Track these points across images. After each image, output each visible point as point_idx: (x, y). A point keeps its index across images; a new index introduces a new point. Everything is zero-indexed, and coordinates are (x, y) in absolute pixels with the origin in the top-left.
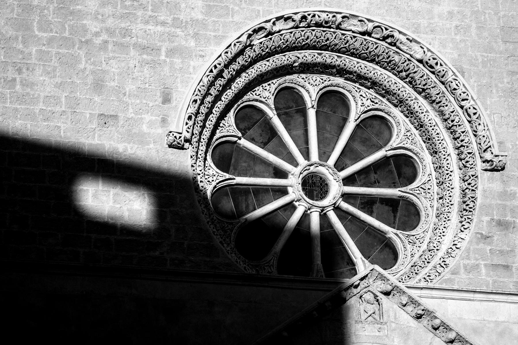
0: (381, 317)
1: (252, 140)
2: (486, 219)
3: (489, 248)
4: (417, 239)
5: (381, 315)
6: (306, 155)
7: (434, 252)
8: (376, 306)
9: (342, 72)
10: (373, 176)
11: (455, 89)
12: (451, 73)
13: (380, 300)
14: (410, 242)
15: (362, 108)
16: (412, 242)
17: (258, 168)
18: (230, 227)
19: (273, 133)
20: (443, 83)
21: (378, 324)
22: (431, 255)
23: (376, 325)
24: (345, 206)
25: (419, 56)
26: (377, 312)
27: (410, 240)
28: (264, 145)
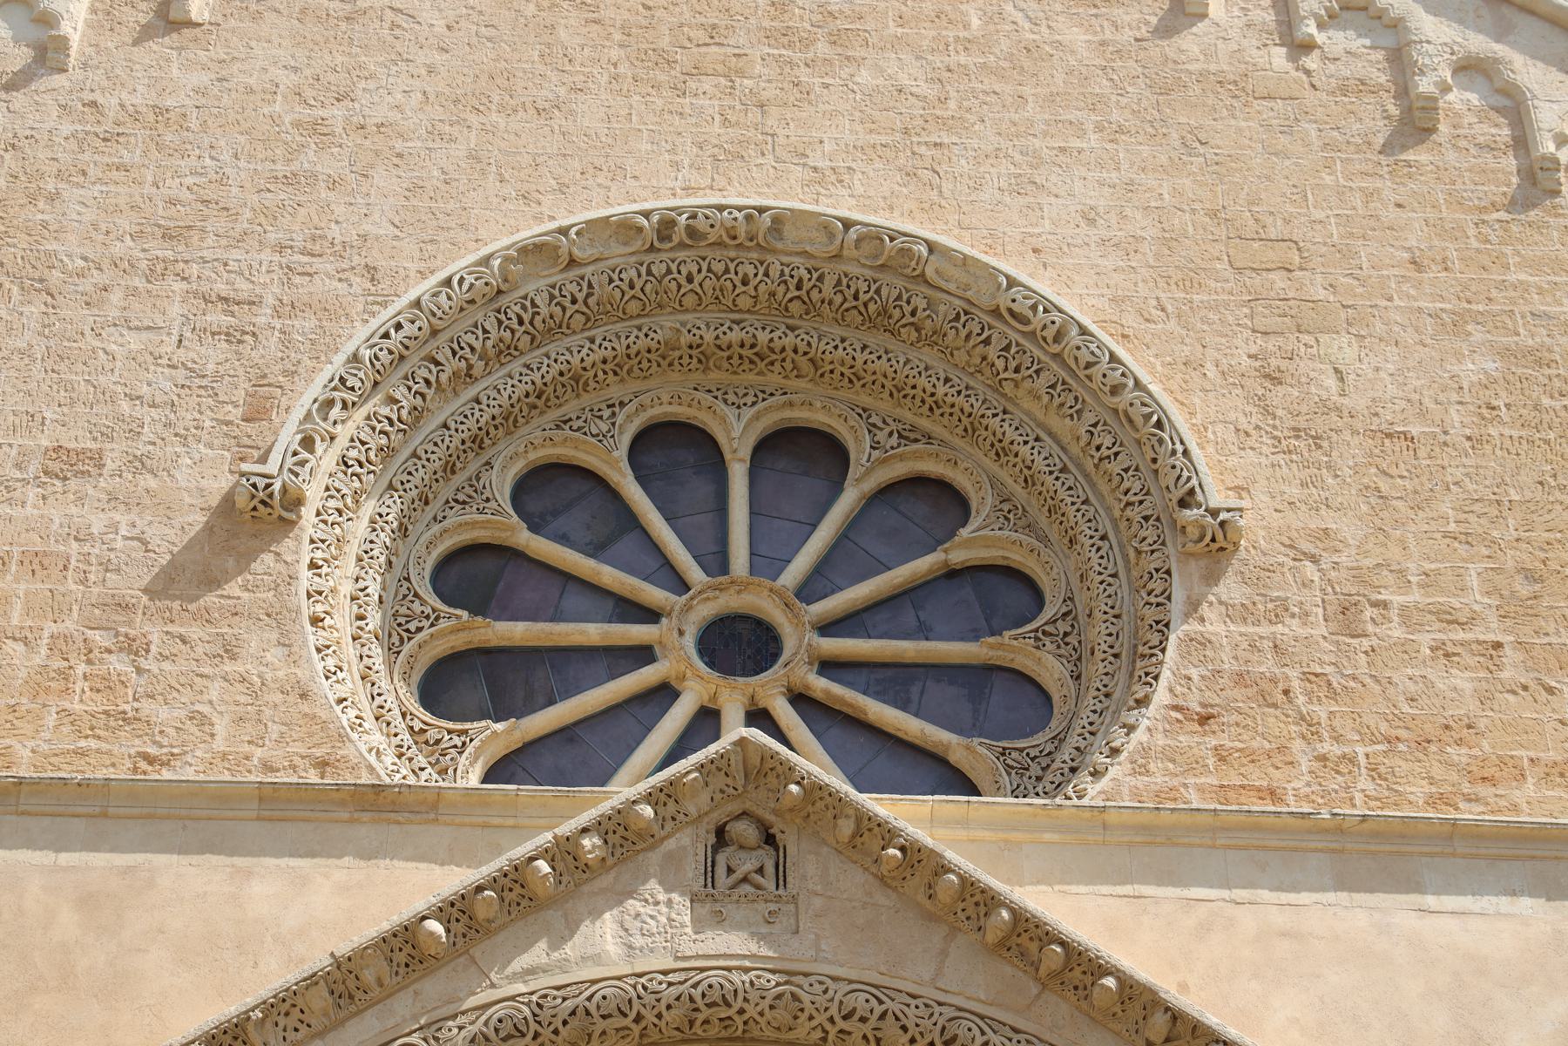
0: (781, 882)
1: (563, 539)
4: (1033, 759)
5: (781, 878)
6: (717, 562)
7: (1062, 774)
8: (766, 857)
10: (909, 618)
11: (1089, 365)
13: (779, 836)
14: (1012, 768)
15: (876, 454)
16: (1015, 765)
17: (573, 600)
18: (457, 741)
19: (629, 521)
20: (1057, 356)
21: (766, 901)
22: (1052, 783)
24: (820, 685)
27: (1009, 762)
28: (595, 550)
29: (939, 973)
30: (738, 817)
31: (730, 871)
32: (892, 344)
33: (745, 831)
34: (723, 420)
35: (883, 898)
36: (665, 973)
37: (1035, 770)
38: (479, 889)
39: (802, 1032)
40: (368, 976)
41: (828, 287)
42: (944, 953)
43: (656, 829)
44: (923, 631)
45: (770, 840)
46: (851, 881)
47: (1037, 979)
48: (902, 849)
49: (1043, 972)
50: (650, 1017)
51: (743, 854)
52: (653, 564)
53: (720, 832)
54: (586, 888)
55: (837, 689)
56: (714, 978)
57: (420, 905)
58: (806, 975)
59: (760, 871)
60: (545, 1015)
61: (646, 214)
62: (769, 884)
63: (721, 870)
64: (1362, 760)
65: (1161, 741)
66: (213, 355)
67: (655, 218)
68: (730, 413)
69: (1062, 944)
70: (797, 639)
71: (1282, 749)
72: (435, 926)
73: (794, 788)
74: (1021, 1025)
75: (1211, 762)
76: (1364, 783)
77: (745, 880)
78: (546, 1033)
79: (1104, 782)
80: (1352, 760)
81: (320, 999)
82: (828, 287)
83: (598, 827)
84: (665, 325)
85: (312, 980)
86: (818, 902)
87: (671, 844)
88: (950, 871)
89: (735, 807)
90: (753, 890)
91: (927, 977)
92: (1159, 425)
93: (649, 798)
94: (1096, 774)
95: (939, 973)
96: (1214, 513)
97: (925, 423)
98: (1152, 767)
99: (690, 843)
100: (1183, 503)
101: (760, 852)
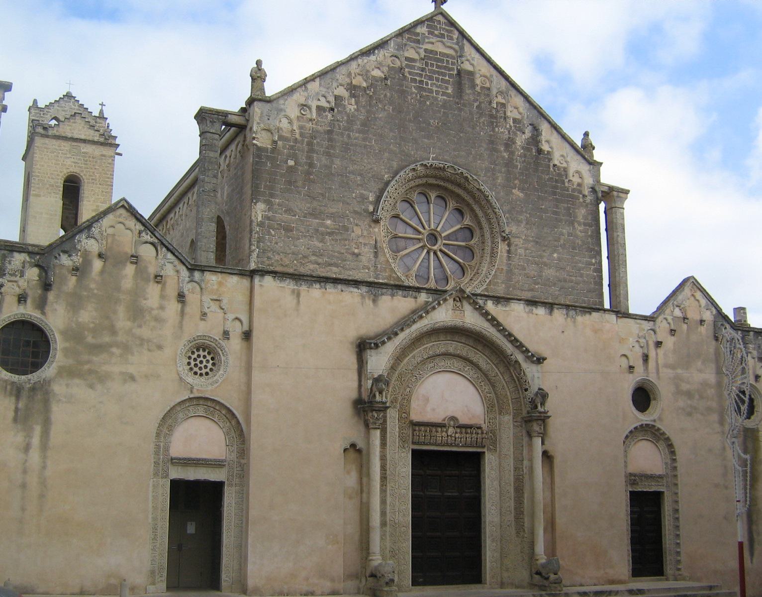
12: (490, 196)
34: (430, 196)
92: (500, 217)
100: (503, 232)
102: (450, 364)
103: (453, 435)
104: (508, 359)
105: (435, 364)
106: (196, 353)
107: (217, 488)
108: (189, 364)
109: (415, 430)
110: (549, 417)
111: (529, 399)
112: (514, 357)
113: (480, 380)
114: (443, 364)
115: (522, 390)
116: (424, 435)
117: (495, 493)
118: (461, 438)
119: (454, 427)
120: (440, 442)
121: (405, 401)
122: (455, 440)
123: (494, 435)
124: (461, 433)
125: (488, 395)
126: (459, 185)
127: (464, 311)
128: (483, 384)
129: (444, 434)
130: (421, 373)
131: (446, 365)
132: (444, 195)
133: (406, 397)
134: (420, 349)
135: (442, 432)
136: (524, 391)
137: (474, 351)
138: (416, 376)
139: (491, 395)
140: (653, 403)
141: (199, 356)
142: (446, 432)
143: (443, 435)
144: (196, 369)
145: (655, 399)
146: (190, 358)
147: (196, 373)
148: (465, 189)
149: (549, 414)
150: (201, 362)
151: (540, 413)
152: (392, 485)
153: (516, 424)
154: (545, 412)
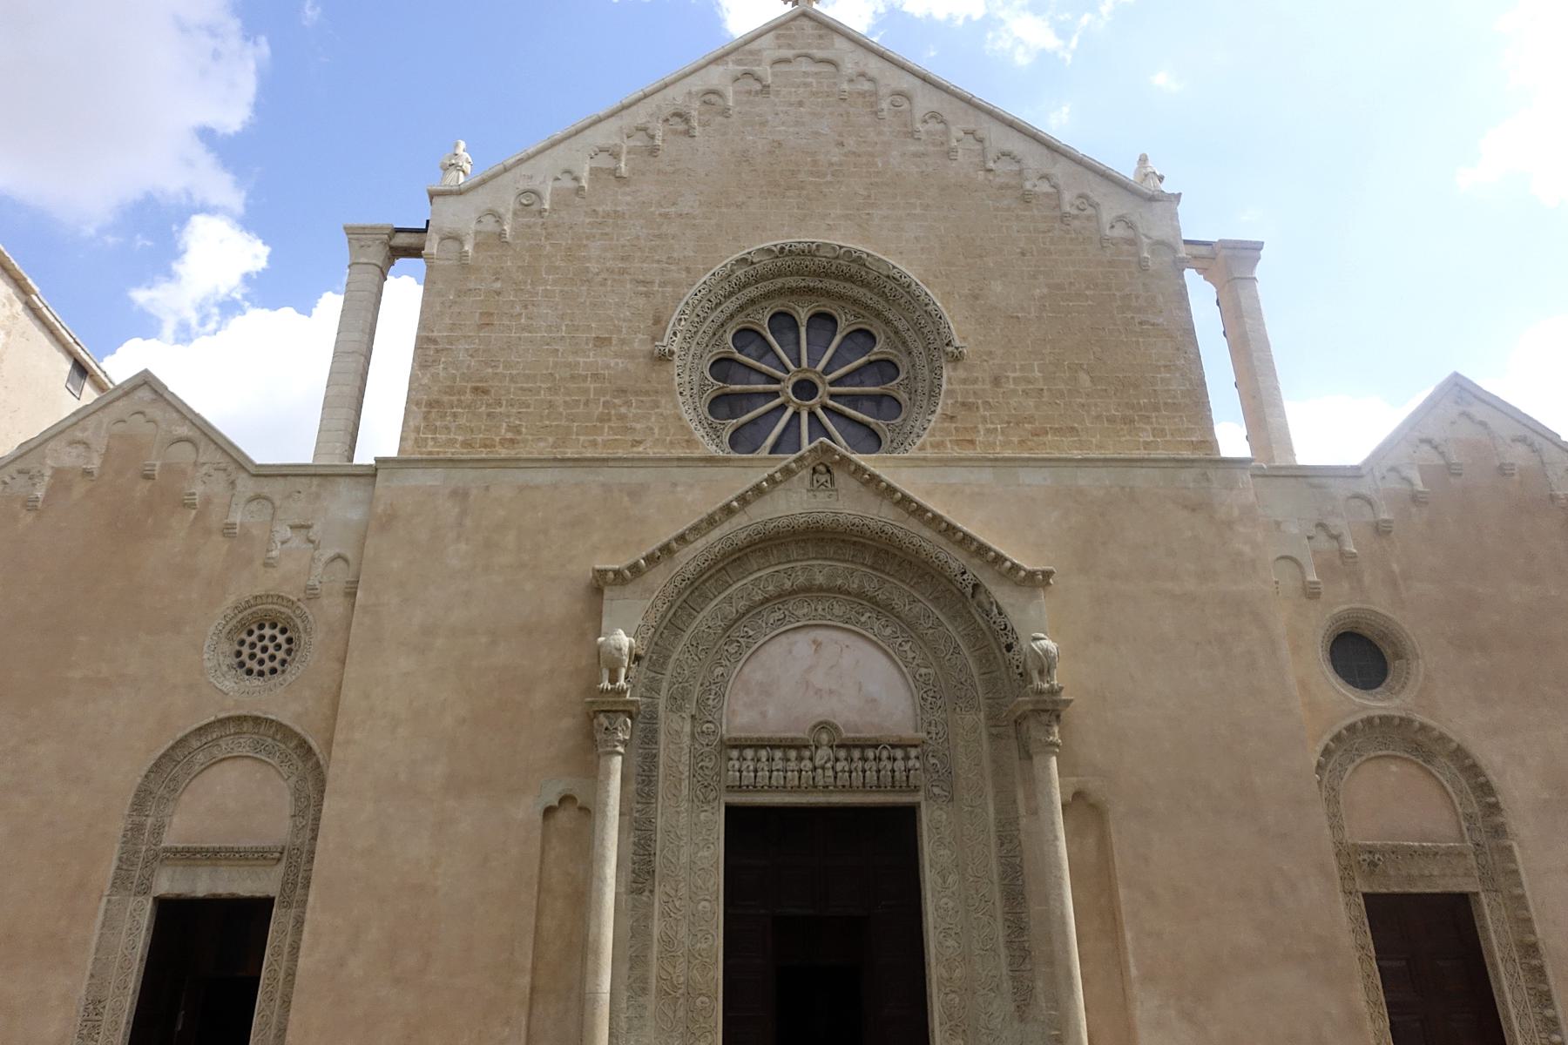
1: (748, 355)
2: (950, 402)
3: (954, 425)
5: (832, 483)
6: (798, 363)
8: (827, 477)
9: (828, 294)
10: (857, 380)
11: (918, 296)
12: (914, 285)
15: (847, 323)
17: (754, 377)
18: (722, 427)
19: (770, 348)
20: (908, 292)
23: (827, 493)
24: (831, 403)
25: (885, 273)
26: (829, 481)
28: (759, 359)
29: (879, 511)
30: (818, 465)
31: (818, 481)
32: (853, 286)
33: (822, 468)
34: (798, 312)
35: (863, 489)
36: (800, 514)
37: (897, 430)
38: (747, 492)
39: (840, 529)
40: (717, 518)
41: (833, 268)
42: (881, 505)
43: (796, 470)
44: (862, 384)
45: (828, 471)
46: (854, 484)
47: (908, 513)
48: (869, 475)
49: (910, 510)
50: (796, 527)
51: (821, 476)
52: (784, 369)
53: (814, 469)
54: (777, 489)
55: (836, 405)
56: (814, 515)
57: (731, 498)
58: (841, 513)
59: (827, 482)
60: (766, 528)
61: (775, 246)
62: (829, 485)
63: (815, 482)
64: (999, 430)
65: (939, 425)
66: (642, 301)
67: (778, 247)
68: (800, 310)
69: (916, 503)
70: (824, 390)
71: (976, 427)
72: (735, 504)
73: (837, 457)
74: (902, 525)
75: (954, 432)
76: (1000, 438)
77: (822, 484)
78: (767, 532)
79: (921, 440)
80: (996, 429)
81: (704, 525)
82: (833, 268)
83: (781, 470)
84: (779, 282)
85: (702, 521)
86: (844, 491)
87: (800, 474)
88: (882, 481)
89: (818, 462)
90: (824, 487)
91: (875, 512)
92: (940, 318)
93: (795, 461)
94: (919, 436)
95: (879, 511)
96: (957, 348)
97: (862, 312)
98: (936, 434)
99: (806, 473)
100: (947, 345)
101: (826, 476)
102: (824, 609)
103: (829, 765)
104: (959, 585)
105: (786, 613)
106: (257, 633)
107: (254, 913)
108: (239, 654)
109: (731, 759)
110: (1068, 702)
111: (1018, 667)
112: (971, 577)
113: (900, 640)
114: (806, 610)
115: (1001, 651)
116: (751, 768)
117: (951, 904)
118: (851, 772)
119: (831, 747)
120: (796, 783)
121: (712, 697)
122: (835, 778)
123: (941, 762)
124: (850, 759)
125: (923, 671)
126: (850, 279)
127: (837, 490)
128: (906, 647)
129: (807, 764)
130: (751, 633)
131: (814, 614)
132: (831, 308)
133: (713, 687)
134: (744, 581)
135: (800, 759)
136: (1004, 650)
137: (876, 576)
138: (738, 642)
139: (931, 671)
140: (1395, 666)
141: (262, 638)
142: (811, 759)
143: (802, 767)
144: (268, 665)
145: (1398, 656)
146: (242, 643)
147: (250, 672)
148: (865, 284)
149: (1064, 696)
150: (264, 649)
151: (1041, 692)
152: (668, 889)
153: (994, 731)
154: (1054, 692)
